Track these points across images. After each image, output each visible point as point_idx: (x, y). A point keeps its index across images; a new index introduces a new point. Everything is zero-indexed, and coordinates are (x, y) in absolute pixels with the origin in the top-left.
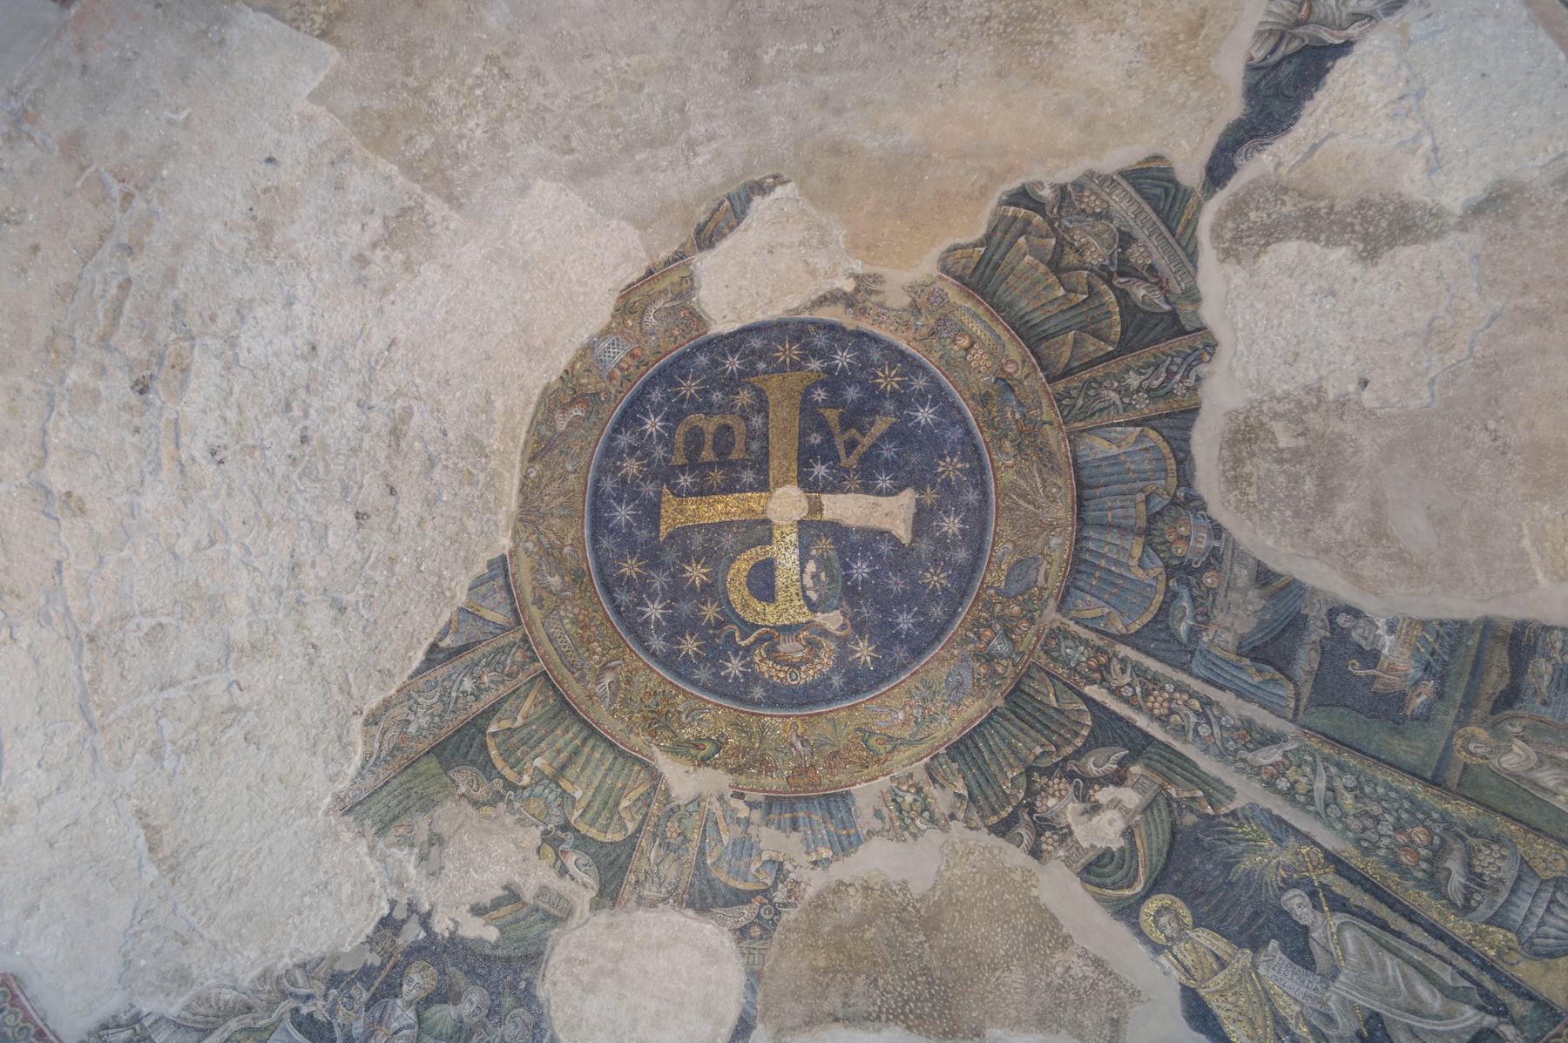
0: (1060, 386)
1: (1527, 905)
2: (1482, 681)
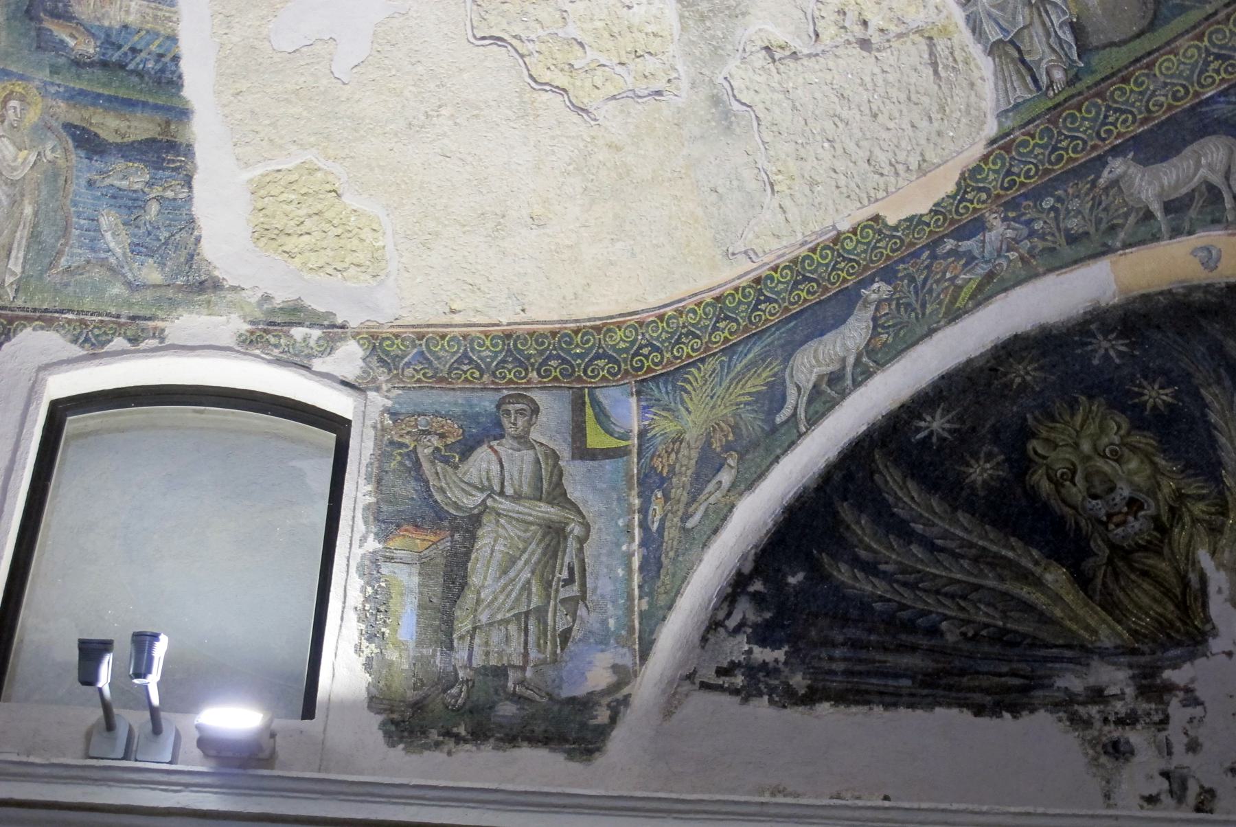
2: (106, 109)
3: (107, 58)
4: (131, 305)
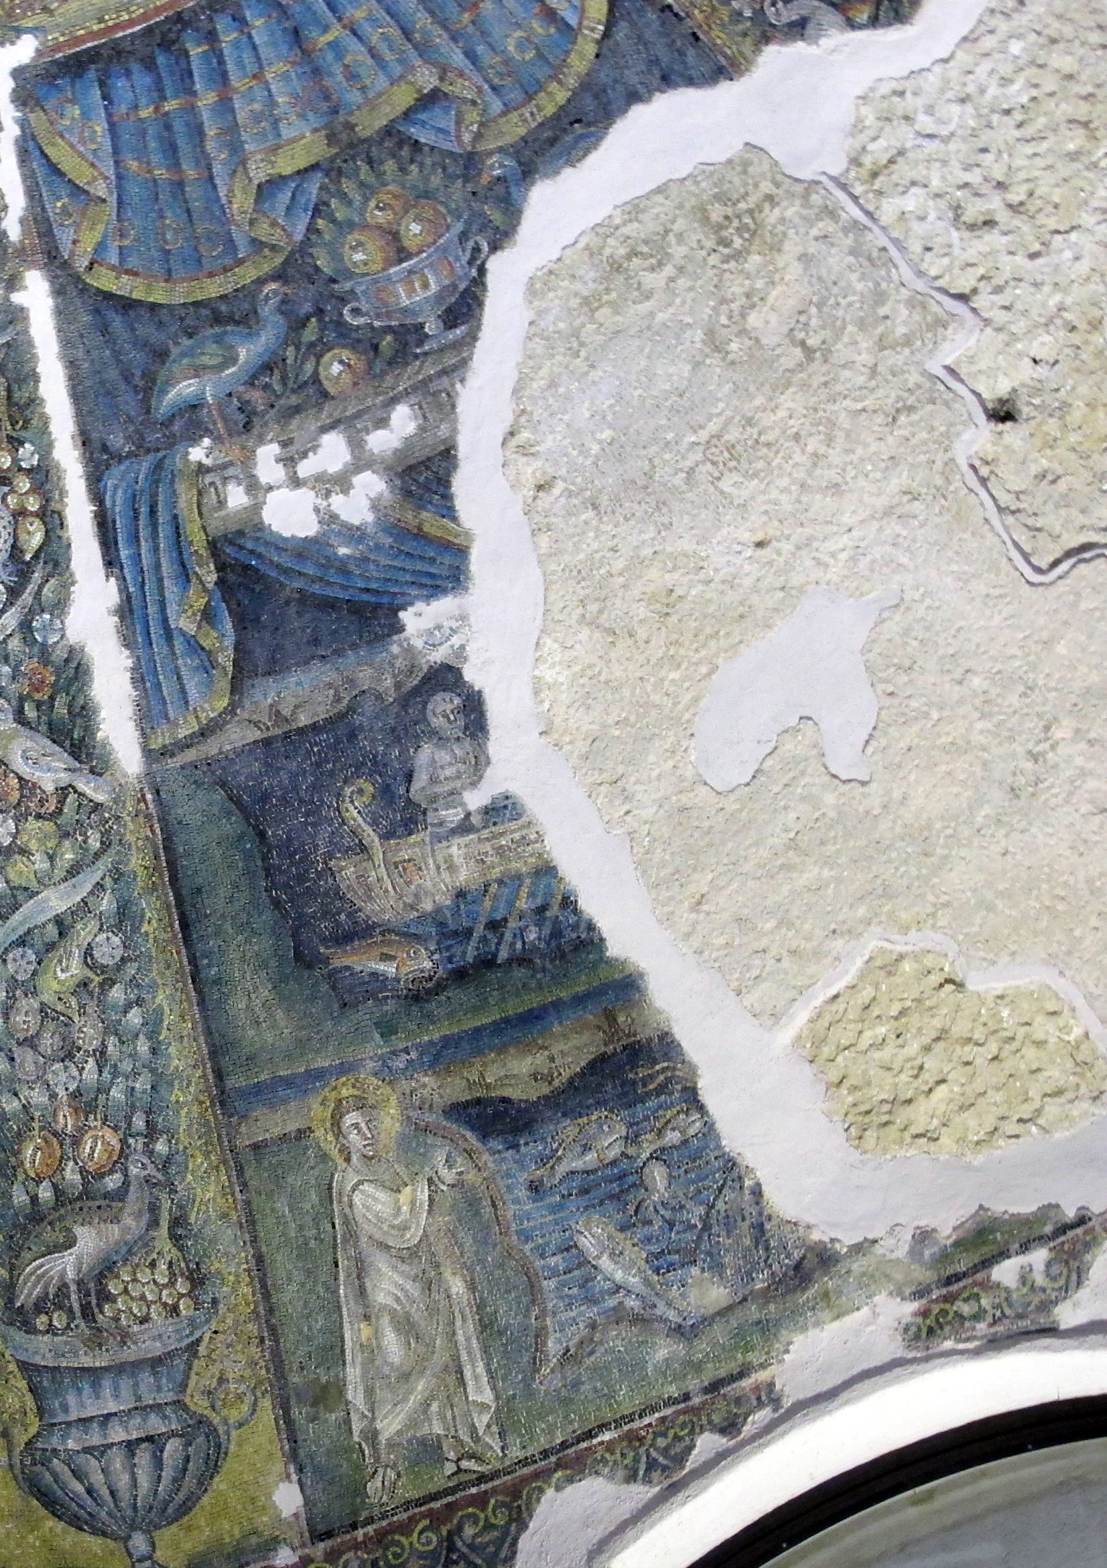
1: (112, 1407)
2: (502, 1050)
3: (458, 962)
4: (698, 1367)
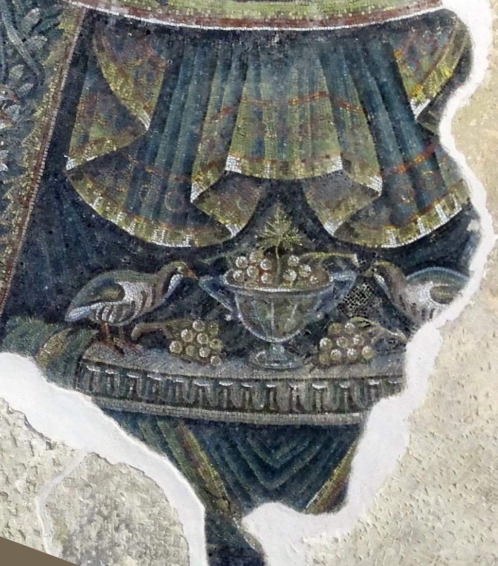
0: (71, 29)
